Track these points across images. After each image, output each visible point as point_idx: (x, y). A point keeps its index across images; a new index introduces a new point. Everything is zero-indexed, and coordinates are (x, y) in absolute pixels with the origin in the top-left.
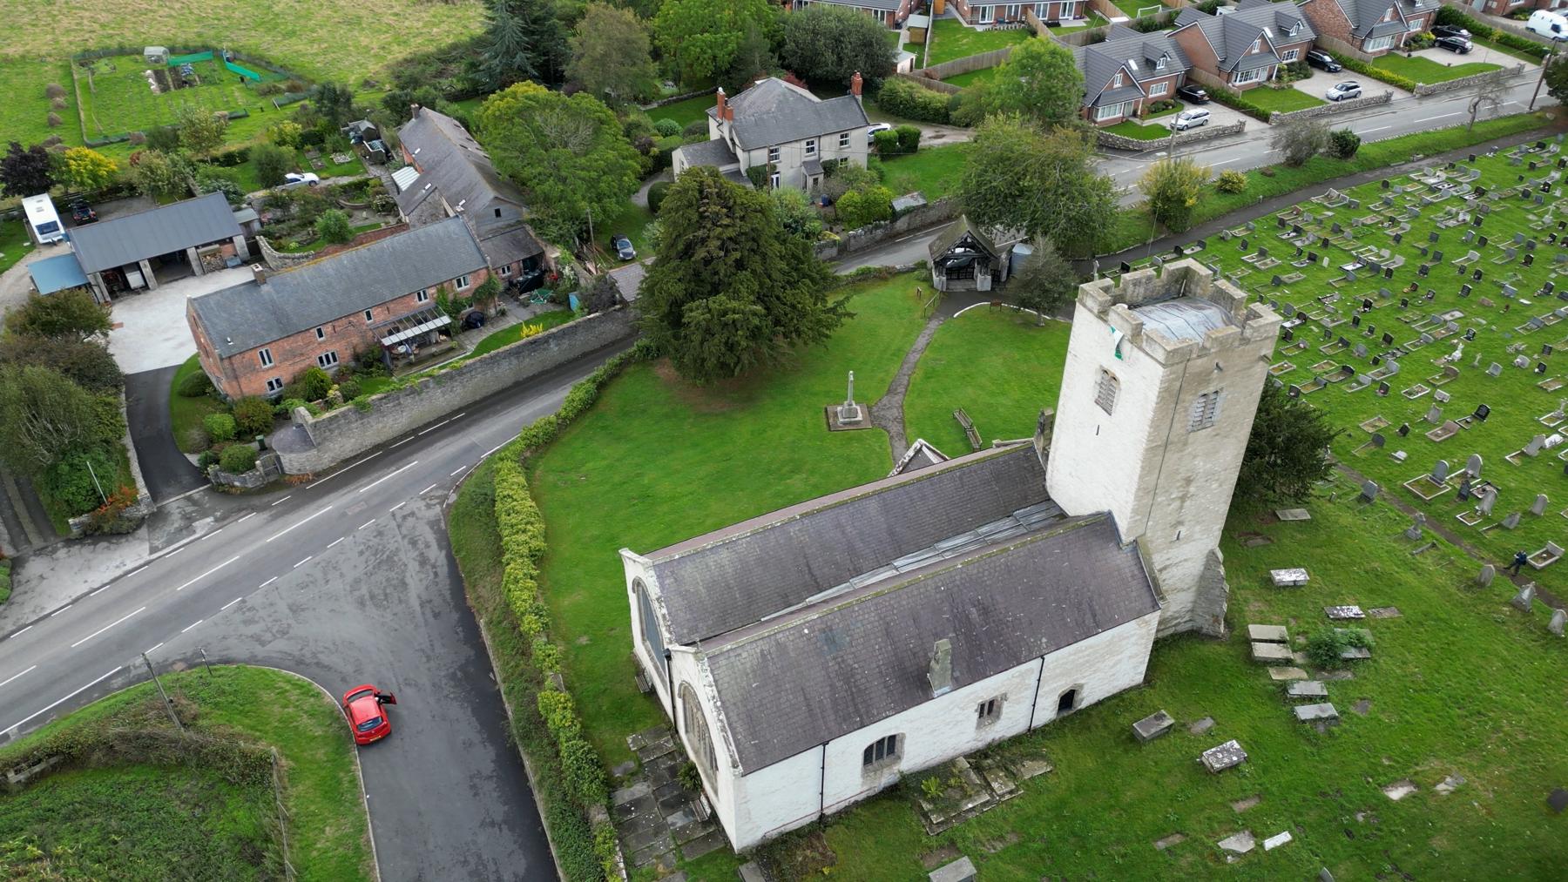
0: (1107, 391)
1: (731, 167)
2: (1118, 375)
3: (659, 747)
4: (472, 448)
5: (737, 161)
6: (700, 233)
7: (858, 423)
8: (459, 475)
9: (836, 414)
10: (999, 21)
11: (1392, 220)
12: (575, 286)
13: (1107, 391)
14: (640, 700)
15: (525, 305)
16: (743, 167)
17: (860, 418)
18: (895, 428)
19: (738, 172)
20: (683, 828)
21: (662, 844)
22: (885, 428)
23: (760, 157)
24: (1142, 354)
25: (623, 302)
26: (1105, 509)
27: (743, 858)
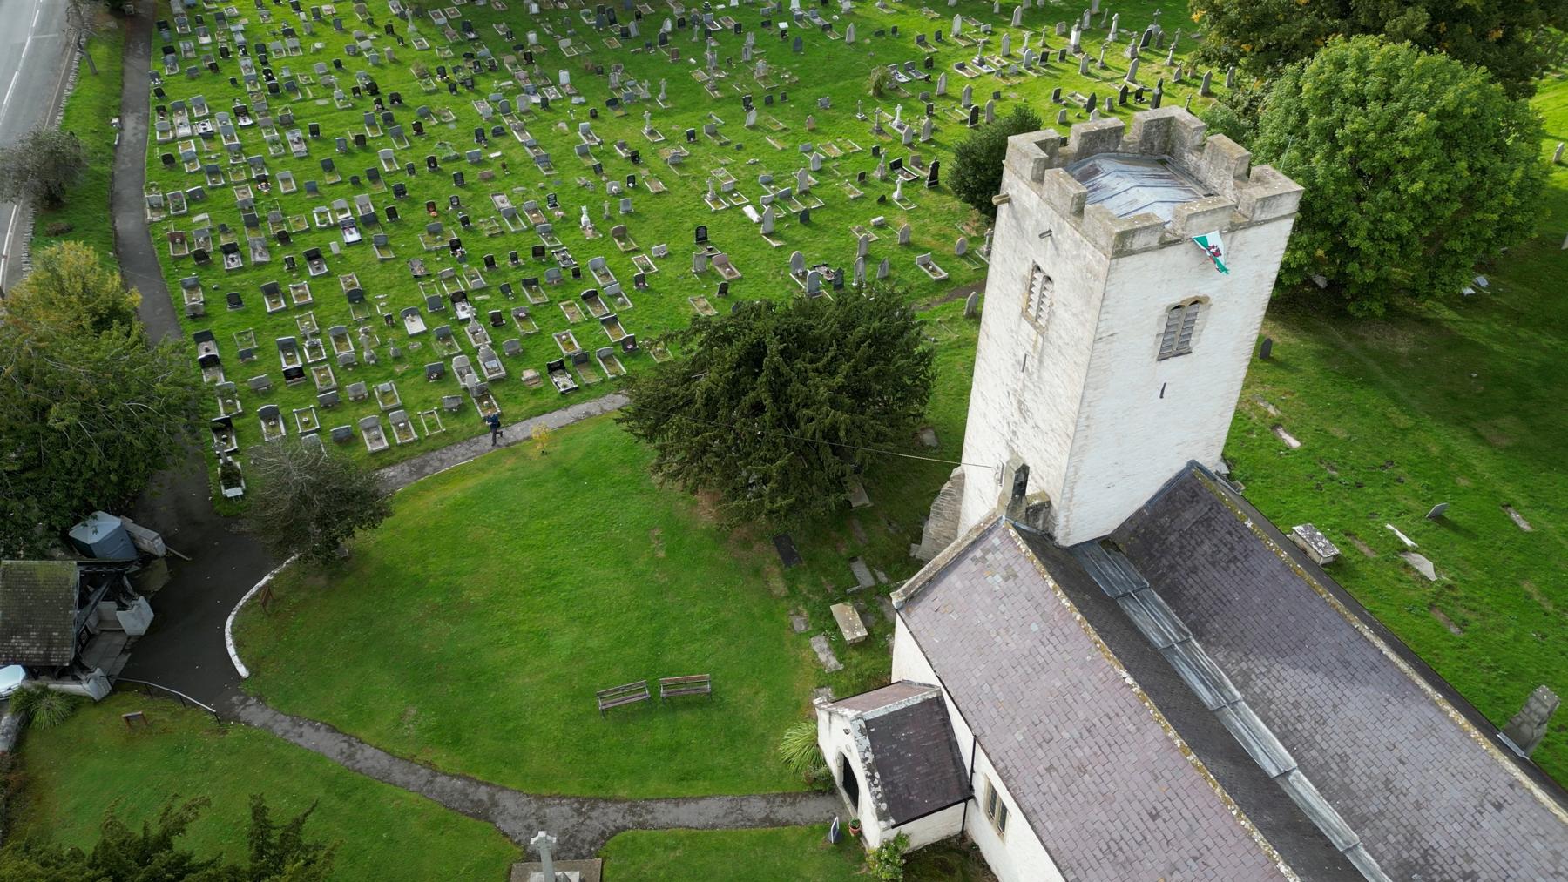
2: (1201, 290)
22: (605, 836)
24: (1251, 232)
26: (1179, 465)
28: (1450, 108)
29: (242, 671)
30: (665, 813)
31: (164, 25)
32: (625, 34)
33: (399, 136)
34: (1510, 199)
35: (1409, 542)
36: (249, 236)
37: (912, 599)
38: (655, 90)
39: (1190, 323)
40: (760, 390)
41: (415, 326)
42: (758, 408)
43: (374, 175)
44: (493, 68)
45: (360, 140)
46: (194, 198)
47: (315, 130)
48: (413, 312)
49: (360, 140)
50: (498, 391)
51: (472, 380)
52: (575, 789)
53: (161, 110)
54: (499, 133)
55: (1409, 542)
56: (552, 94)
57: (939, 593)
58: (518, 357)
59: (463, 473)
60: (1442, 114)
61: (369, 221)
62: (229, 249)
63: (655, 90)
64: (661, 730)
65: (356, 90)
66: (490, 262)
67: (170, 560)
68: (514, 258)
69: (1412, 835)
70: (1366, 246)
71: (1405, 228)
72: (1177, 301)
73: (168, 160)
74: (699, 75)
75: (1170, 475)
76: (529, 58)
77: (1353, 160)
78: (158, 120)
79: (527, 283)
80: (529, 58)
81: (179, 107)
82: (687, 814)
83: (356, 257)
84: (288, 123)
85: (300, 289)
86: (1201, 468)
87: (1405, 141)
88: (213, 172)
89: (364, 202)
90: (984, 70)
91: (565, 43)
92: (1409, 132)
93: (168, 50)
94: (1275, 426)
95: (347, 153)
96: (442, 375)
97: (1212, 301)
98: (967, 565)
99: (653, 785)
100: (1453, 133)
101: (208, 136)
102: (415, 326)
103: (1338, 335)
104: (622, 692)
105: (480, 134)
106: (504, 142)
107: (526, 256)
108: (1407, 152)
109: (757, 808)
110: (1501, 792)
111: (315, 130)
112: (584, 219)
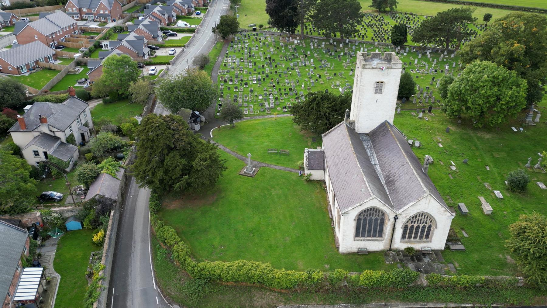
0: (379, 87)
1: (59, 142)
2: (383, 80)
3: (394, 256)
4: (145, 292)
5: (59, 138)
6: (176, 136)
7: (255, 171)
8: (161, 300)
9: (245, 173)
10: (29, 70)
11: (241, 71)
12: (65, 220)
13: (379, 87)
14: (367, 257)
15: (42, 246)
16: (64, 140)
17: (254, 169)
18: (264, 165)
19: (62, 143)
20: (431, 259)
21: (436, 266)
23: (68, 132)
24: (392, 70)
25: (115, 201)
26: (384, 121)
27: (447, 247)
28: (496, 76)
29: (212, 136)
30: (272, 166)
31: (232, 42)
32: (331, 55)
33: (271, 67)
34: (508, 98)
35: (453, 164)
36: (235, 79)
37: (325, 136)
38: (331, 66)
39: (381, 87)
40: (315, 105)
41: (261, 97)
42: (313, 108)
43: (263, 73)
44: (297, 57)
45: (263, 66)
46: (227, 72)
47: (255, 64)
48: (261, 95)
49: (263, 66)
50: (272, 110)
51: (267, 106)
52: (259, 160)
53: (227, 57)
54: (293, 69)
55: (453, 164)
56: (308, 64)
57: (330, 135)
58: (278, 105)
59: (260, 120)
60: (494, 77)
61: (259, 80)
62: (231, 81)
63: (331, 66)
64: (277, 157)
65: (266, 58)
66: (280, 90)
67: (205, 122)
68: (285, 90)
69: (390, 171)
70: (470, 105)
71: (481, 102)
72: (378, 81)
73: (225, 65)
74: (344, 64)
75: (381, 122)
76: (306, 56)
77: (472, 86)
78: (225, 58)
79: (285, 94)
80: (306, 56)
81: (230, 57)
82: (276, 167)
83: (254, 86)
84: (250, 62)
85: (241, 89)
86: (388, 122)
87: (482, 82)
88: (233, 68)
89: (259, 77)
90: (418, 72)
91: (316, 55)
92: (482, 79)
93: (232, 47)
94: (439, 143)
95: (260, 69)
96: (262, 105)
97: (386, 82)
98: (336, 130)
99: (272, 163)
100: (495, 82)
101: (234, 62)
102: (261, 97)
103: (471, 132)
104: (272, 150)
105: (288, 69)
106: (293, 71)
107: (287, 90)
108: (482, 84)
109: (289, 169)
110: (405, 163)
111: (255, 64)
112: (303, 86)
